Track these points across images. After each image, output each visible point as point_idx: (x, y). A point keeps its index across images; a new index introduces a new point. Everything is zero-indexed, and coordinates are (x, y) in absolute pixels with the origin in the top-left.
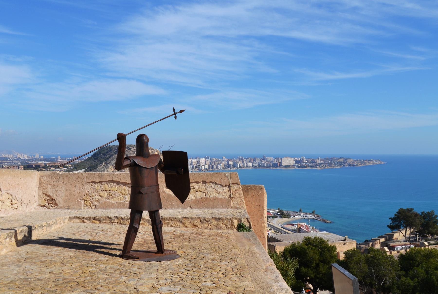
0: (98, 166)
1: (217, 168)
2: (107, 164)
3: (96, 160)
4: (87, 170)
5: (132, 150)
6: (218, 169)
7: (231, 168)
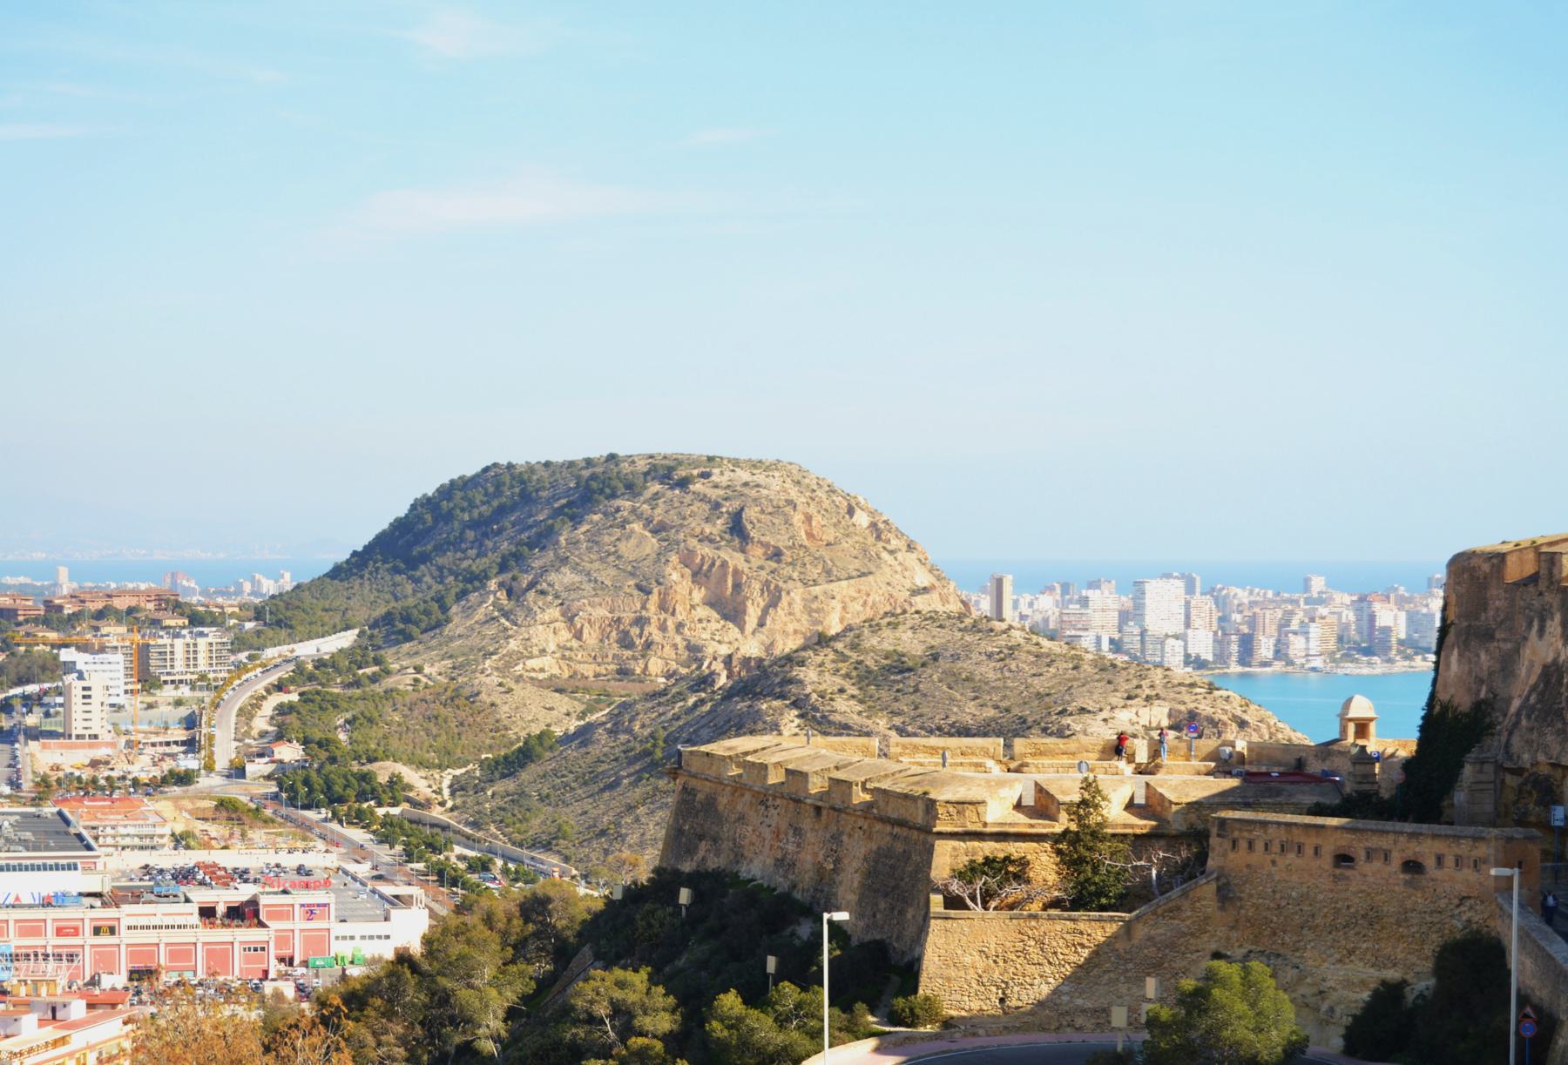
0: (454, 609)
1: (1280, 653)
3: (422, 567)
5: (697, 487)
6: (1290, 663)
7: (1390, 661)
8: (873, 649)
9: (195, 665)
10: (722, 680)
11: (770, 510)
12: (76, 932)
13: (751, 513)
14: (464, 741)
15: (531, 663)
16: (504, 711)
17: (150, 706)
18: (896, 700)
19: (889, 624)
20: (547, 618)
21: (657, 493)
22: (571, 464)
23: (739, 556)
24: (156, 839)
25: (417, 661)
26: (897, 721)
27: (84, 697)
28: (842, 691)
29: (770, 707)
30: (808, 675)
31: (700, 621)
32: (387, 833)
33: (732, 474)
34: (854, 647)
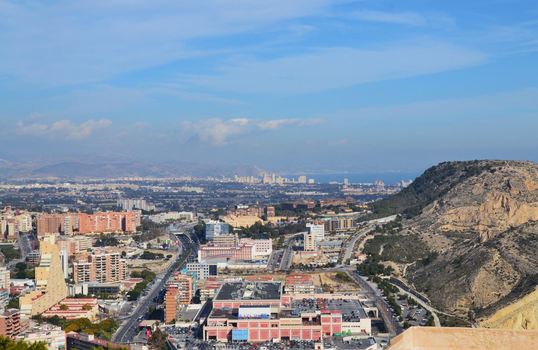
2: (441, 204)
4: (400, 217)
8: (525, 233)
9: (347, 227)
10: (485, 240)
11: (518, 179)
12: (267, 326)
13: (512, 181)
14: (416, 253)
15: (443, 227)
16: (429, 244)
17: (331, 240)
18: (529, 249)
19: (532, 224)
20: (450, 212)
21: (485, 174)
22: (465, 163)
23: (508, 194)
24: (310, 289)
25: (411, 225)
26: (528, 256)
27: (309, 239)
28: (514, 246)
29: (491, 251)
30: (504, 241)
31: (496, 213)
32: (382, 285)
33: (508, 168)
34: (520, 232)
